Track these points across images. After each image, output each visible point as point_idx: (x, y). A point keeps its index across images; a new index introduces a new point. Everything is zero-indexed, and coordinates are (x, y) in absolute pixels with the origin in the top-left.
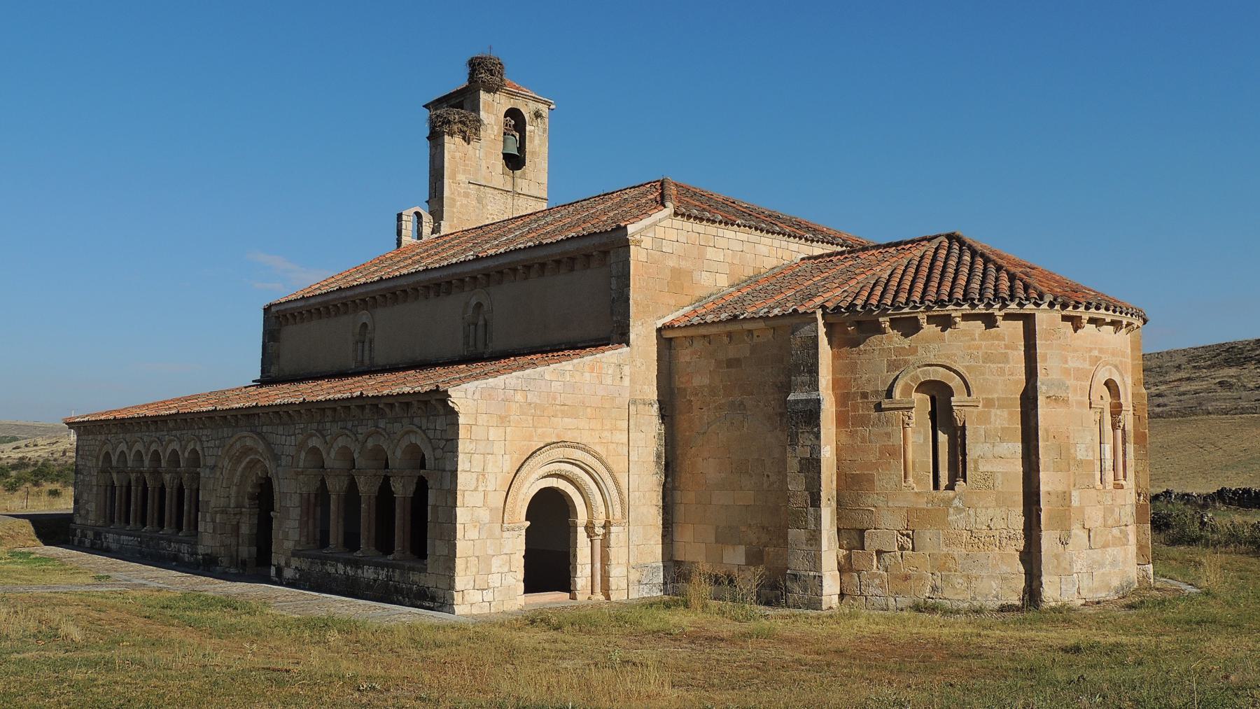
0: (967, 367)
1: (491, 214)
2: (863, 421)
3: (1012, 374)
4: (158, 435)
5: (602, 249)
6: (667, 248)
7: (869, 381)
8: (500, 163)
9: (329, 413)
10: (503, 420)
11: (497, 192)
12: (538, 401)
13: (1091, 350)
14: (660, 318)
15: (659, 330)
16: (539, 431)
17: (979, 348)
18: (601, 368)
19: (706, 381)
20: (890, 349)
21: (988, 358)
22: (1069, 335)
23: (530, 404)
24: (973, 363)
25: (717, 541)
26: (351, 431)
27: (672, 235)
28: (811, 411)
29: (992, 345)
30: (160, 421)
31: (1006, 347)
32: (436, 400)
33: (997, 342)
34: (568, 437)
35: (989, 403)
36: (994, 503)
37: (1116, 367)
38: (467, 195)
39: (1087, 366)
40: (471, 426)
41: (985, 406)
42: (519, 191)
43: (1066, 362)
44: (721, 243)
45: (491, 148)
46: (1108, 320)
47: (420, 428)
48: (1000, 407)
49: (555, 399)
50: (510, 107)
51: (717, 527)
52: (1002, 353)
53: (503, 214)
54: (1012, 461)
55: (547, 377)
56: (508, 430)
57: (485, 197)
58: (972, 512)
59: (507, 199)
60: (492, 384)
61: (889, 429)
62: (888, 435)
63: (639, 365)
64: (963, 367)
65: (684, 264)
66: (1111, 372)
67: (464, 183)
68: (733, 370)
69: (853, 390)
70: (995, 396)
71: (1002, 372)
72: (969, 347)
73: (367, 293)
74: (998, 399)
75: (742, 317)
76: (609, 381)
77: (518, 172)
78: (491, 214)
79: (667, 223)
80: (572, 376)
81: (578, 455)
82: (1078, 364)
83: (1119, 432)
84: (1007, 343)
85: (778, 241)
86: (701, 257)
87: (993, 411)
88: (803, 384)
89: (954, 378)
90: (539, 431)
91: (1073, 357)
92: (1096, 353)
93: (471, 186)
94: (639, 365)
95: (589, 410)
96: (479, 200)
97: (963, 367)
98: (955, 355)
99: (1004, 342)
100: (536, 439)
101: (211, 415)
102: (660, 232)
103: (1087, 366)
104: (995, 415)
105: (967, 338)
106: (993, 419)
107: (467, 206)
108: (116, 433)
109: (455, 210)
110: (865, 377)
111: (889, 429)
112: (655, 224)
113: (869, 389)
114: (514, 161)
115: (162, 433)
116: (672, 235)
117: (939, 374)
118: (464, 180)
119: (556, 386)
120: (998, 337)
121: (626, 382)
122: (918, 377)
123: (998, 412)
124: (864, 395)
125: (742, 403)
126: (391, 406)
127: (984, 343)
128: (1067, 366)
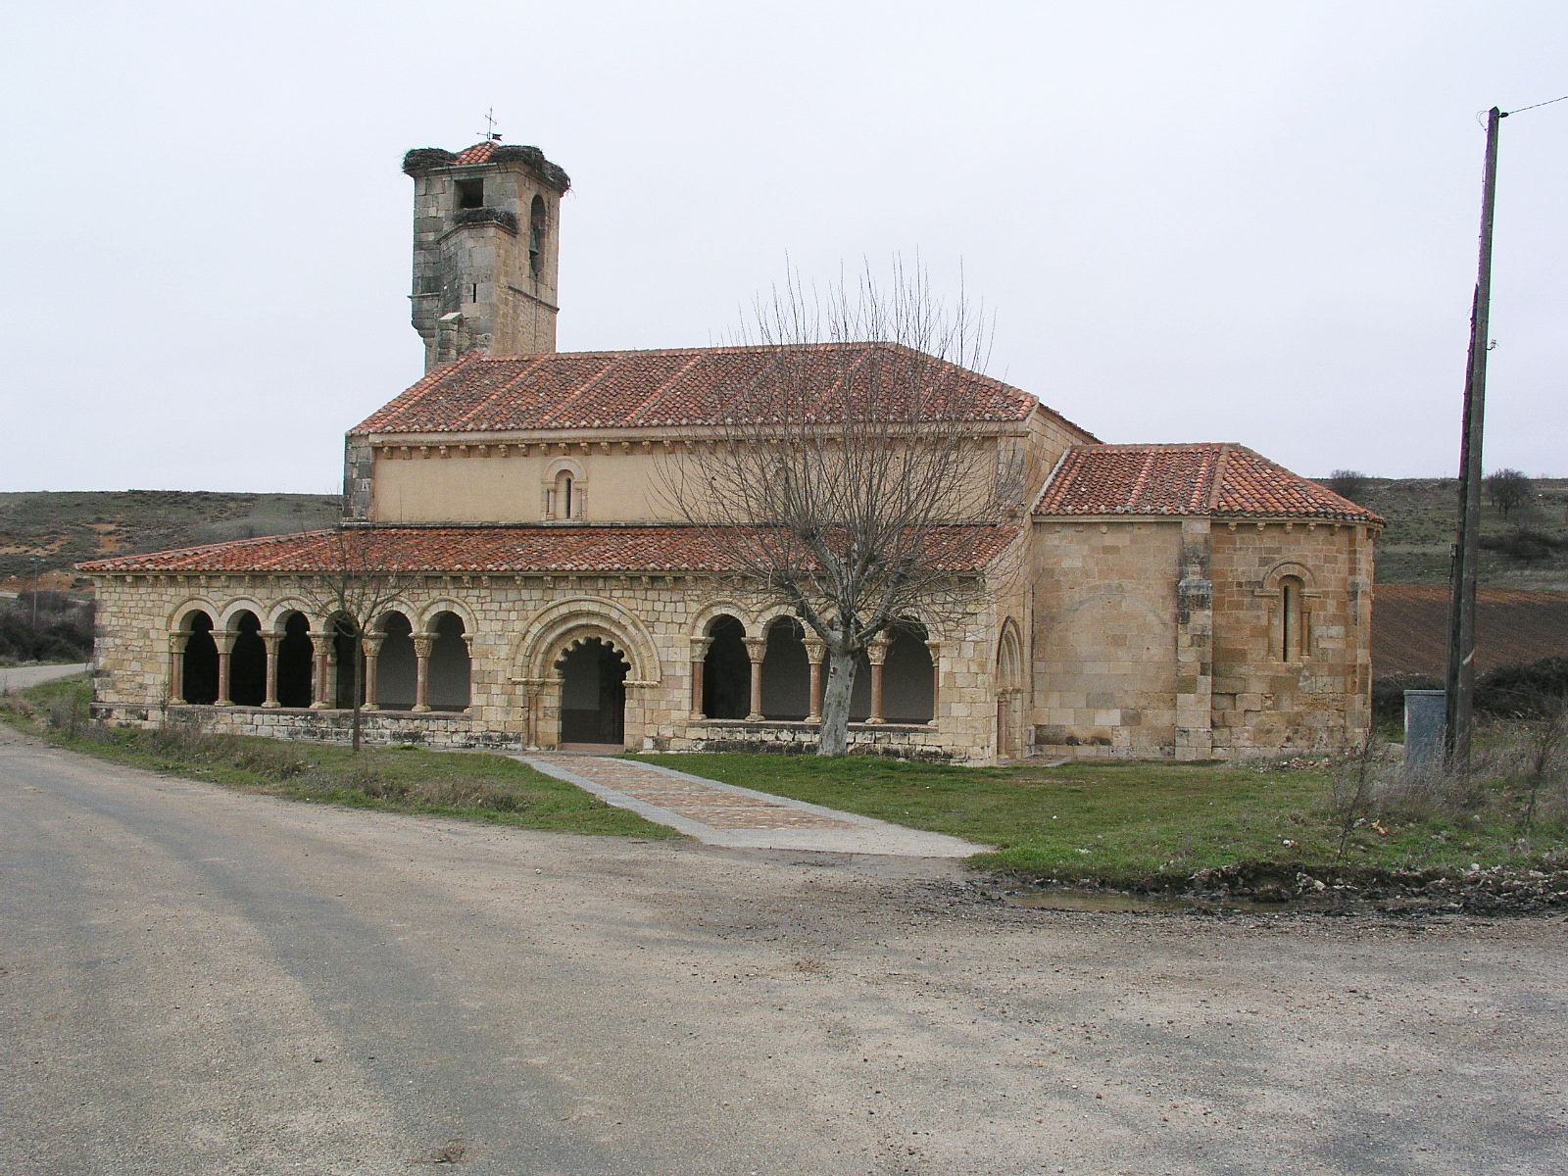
21: (1327, 560)
25: (1088, 706)
28: (1203, 596)
31: (1337, 552)
36: (1327, 673)
51: (1088, 694)
58: (1313, 679)
61: (1260, 613)
62: (1258, 617)
68: (1110, 557)
96: (515, 308)
98: (1307, 556)
110: (1240, 569)
117: (1294, 571)
124: (1240, 585)
127: (1324, 547)
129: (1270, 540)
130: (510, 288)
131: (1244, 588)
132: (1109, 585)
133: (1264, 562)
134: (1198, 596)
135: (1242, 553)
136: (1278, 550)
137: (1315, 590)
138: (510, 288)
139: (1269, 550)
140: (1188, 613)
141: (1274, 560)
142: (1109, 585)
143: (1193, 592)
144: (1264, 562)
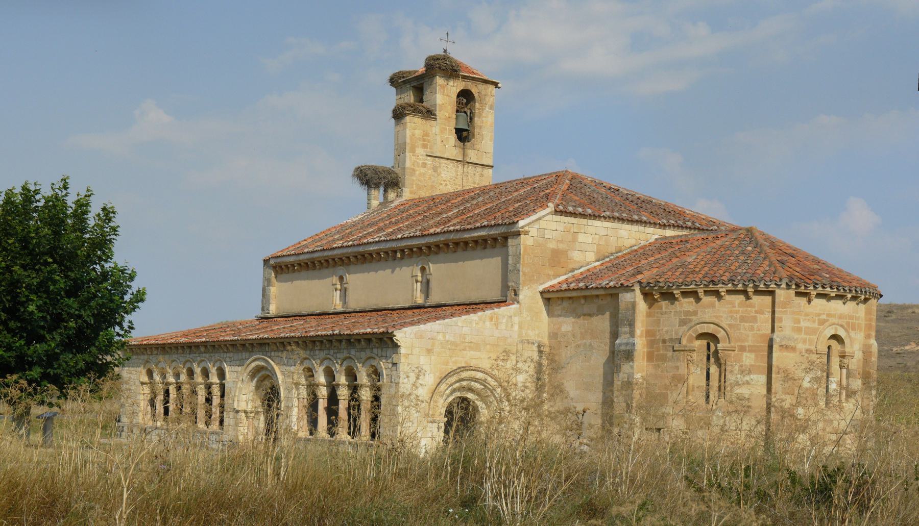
0: (730, 325)
1: (444, 181)
2: (663, 358)
3: (759, 330)
4: (191, 356)
5: (503, 236)
6: (548, 235)
7: (667, 332)
8: (453, 138)
9: (318, 344)
10: (429, 351)
11: (449, 161)
12: (453, 340)
13: (819, 315)
14: (541, 284)
15: (541, 293)
16: (454, 359)
17: (737, 312)
18: (497, 319)
19: (570, 329)
20: (681, 312)
21: (743, 319)
22: (803, 305)
23: (448, 341)
24: (733, 322)
26: (333, 356)
27: (553, 226)
28: (629, 350)
29: (746, 310)
30: (195, 346)
31: (756, 312)
32: (387, 338)
33: (749, 309)
34: (473, 363)
35: (742, 349)
37: (842, 326)
38: (424, 165)
39: (816, 325)
40: (408, 354)
41: (739, 350)
42: (468, 161)
43: (799, 322)
44: (591, 230)
45: (445, 125)
46: (833, 294)
47: (377, 355)
48: (750, 351)
49: (465, 339)
50: (462, 88)
52: (752, 316)
53: (454, 180)
54: (756, 386)
55: (460, 324)
56: (433, 358)
57: (440, 167)
59: (458, 167)
60: (423, 329)
61: (679, 364)
62: (677, 368)
63: (525, 316)
64: (727, 324)
65: (561, 246)
66: (836, 329)
67: (422, 155)
69: (658, 338)
70: (746, 344)
71: (752, 329)
72: (731, 312)
73: (343, 254)
74: (749, 346)
75: (591, 286)
76: (504, 328)
77: (467, 144)
78: (444, 181)
79: (550, 217)
80: (477, 324)
82: (808, 324)
83: (844, 371)
84: (756, 309)
85: (635, 228)
86: (574, 240)
87: (745, 354)
88: (625, 333)
89: (721, 331)
90: (454, 359)
91: (805, 319)
92: (824, 317)
93: (429, 158)
94: (525, 316)
95: (488, 346)
96: (435, 169)
97: (727, 324)
98: (722, 317)
99: (754, 309)
100: (451, 364)
101: (234, 343)
102: (543, 224)
103: (816, 325)
104: (746, 356)
105: (730, 306)
106: (744, 359)
107: (424, 174)
108: (157, 354)
109: (415, 178)
111: (679, 364)
112: (540, 219)
113: (667, 337)
114: (463, 135)
115: (194, 355)
116: (553, 226)
117: (711, 329)
118: (422, 153)
119: (466, 330)
120: (751, 306)
121: (516, 328)
122: (697, 330)
123: (748, 354)
124: (664, 341)
125: (590, 345)
126: (359, 341)
127: (741, 309)
128: (799, 325)
129: (687, 304)
130: (427, 155)
131: (668, 344)
132: (585, 344)
133: (683, 323)
134: (625, 351)
135: (666, 316)
136: (695, 313)
137: (729, 345)
138: (427, 155)
139: (687, 313)
140: (620, 365)
141: (690, 321)
142: (585, 344)
143: (623, 348)
144: (683, 323)
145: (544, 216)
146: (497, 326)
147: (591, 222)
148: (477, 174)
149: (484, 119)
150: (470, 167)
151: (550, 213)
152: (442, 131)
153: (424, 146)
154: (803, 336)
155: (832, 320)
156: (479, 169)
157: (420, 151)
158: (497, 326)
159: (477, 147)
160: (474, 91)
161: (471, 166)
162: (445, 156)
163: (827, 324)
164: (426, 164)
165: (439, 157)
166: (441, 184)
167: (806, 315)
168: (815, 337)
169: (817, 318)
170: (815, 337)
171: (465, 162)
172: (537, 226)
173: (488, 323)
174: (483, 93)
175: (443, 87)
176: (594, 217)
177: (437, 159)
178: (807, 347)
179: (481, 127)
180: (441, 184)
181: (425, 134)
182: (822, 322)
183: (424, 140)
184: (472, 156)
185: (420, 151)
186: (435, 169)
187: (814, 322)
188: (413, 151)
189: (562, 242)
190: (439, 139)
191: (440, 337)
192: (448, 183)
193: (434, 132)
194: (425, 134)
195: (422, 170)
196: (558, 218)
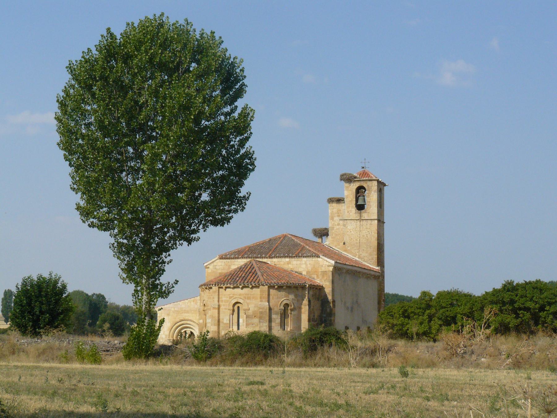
13: (230, 295)
18: (196, 301)
27: (220, 264)
38: (339, 224)
39: (228, 299)
50: (358, 186)
55: (181, 304)
81: (189, 322)
90: (178, 317)
92: (232, 295)
96: (344, 225)
102: (215, 264)
103: (228, 299)
107: (339, 228)
109: (333, 231)
112: (213, 262)
114: (360, 207)
116: (220, 264)
119: (183, 306)
145: (215, 261)
146: (196, 304)
147: (236, 260)
148: (368, 224)
149: (371, 198)
150: (364, 222)
151: (218, 259)
152: (348, 207)
153: (339, 216)
154: (224, 303)
155: (235, 297)
156: (369, 222)
157: (336, 218)
158: (196, 304)
159: (368, 211)
160: (365, 186)
161: (364, 221)
162: (350, 219)
163: (233, 298)
164: (339, 224)
165: (346, 220)
166: (348, 232)
167: (225, 295)
168: (228, 304)
169: (228, 296)
170: (228, 304)
171: (361, 220)
172: (212, 265)
173: (192, 303)
174: (370, 186)
175: (347, 187)
176: (238, 258)
177: (345, 221)
178: (225, 307)
179: (369, 202)
180: (348, 232)
181: (339, 210)
182: (230, 298)
183: (338, 213)
184: (365, 215)
185: (336, 218)
186: (344, 225)
187: (227, 297)
188: (332, 219)
189: (224, 269)
190: (346, 211)
191: (173, 309)
192: (352, 231)
193: (343, 208)
194: (339, 210)
195: (338, 227)
196: (222, 260)
